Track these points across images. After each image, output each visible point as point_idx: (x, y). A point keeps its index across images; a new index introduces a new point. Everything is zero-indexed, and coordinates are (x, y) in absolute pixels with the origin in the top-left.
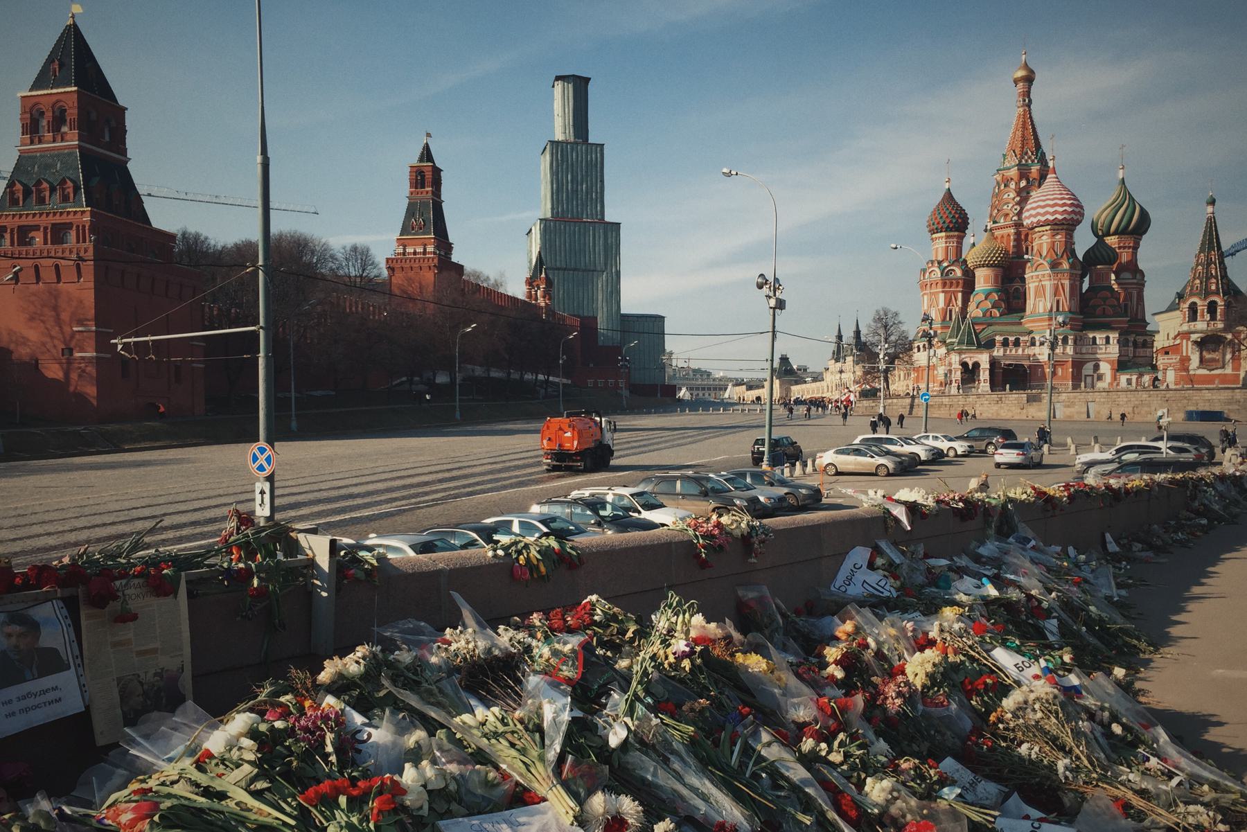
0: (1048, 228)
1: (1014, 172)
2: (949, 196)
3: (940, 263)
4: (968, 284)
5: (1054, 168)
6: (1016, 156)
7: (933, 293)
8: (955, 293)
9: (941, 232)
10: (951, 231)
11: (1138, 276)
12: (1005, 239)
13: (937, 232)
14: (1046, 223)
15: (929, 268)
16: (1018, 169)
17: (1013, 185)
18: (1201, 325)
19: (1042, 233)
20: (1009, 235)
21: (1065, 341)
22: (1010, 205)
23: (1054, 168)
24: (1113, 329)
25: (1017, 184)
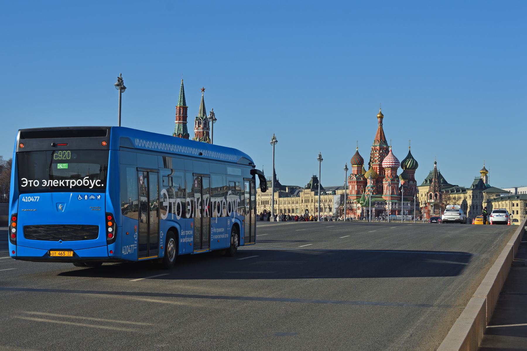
0: (390, 169)
1: (378, 147)
2: (357, 153)
3: (356, 175)
4: (365, 183)
5: (391, 150)
6: (379, 142)
7: (353, 185)
8: (361, 185)
9: (356, 165)
10: (359, 165)
11: (415, 183)
12: (375, 168)
13: (354, 165)
14: (390, 167)
15: (352, 176)
16: (379, 147)
17: (378, 152)
18: (433, 201)
19: (388, 170)
20: (377, 168)
21: (396, 203)
22: (377, 158)
23: (391, 150)
24: (409, 201)
25: (379, 151)
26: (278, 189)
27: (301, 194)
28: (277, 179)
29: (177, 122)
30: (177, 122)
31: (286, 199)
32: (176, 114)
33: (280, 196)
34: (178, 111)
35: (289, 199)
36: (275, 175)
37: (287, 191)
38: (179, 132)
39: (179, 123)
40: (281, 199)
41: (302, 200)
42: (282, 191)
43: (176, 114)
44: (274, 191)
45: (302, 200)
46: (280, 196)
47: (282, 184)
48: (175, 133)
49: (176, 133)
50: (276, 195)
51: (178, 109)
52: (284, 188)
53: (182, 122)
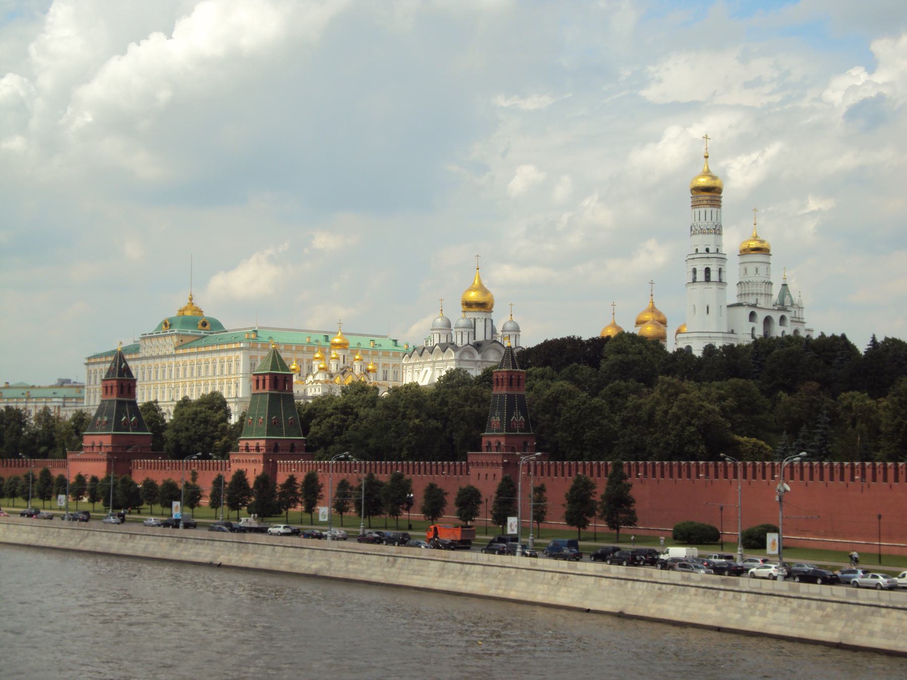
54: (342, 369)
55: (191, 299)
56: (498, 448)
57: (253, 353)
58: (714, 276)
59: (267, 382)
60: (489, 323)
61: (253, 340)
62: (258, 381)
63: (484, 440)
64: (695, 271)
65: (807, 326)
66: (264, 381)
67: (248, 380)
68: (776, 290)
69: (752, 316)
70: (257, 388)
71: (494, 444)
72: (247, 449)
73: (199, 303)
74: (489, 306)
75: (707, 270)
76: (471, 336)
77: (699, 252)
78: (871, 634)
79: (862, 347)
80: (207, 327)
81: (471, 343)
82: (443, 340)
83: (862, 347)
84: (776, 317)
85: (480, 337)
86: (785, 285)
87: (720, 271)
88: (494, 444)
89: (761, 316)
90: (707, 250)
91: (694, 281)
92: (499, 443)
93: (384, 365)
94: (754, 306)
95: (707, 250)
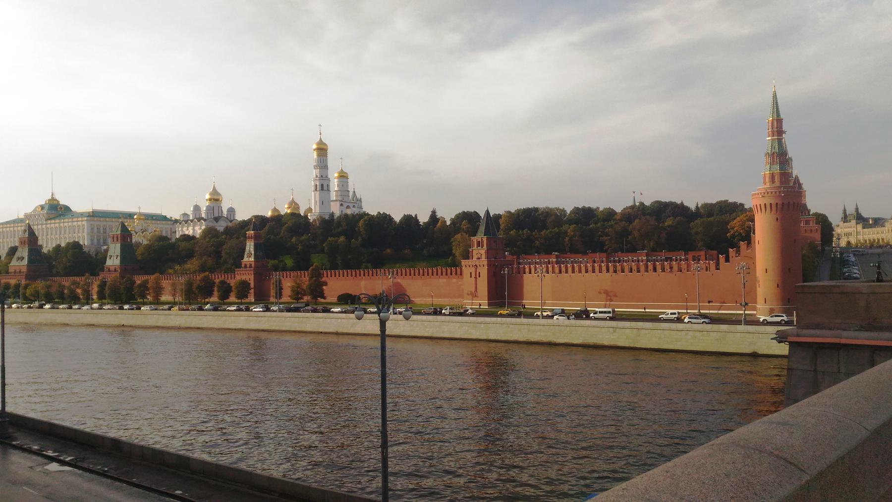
26: (862, 221)
27: (886, 224)
28: (860, 212)
29: (770, 138)
30: (770, 138)
31: (870, 230)
32: (768, 129)
33: (864, 228)
34: (770, 124)
35: (873, 229)
36: (857, 209)
37: (871, 223)
38: (773, 151)
39: (772, 139)
40: (866, 230)
41: (889, 230)
42: (866, 223)
43: (768, 129)
44: (857, 223)
45: (889, 230)
46: (864, 228)
47: (865, 216)
48: (768, 153)
49: (770, 152)
50: (860, 227)
51: (770, 122)
52: (866, 220)
53: (776, 137)
54: (141, 230)
55: (52, 195)
56: (251, 266)
57: (92, 223)
58: (325, 188)
59: (119, 238)
60: (220, 208)
61: (95, 215)
62: (113, 237)
63: (243, 263)
64: (316, 186)
65: (364, 210)
66: (117, 237)
67: (89, 236)
68: (351, 194)
69: (341, 205)
70: (113, 241)
71: (248, 266)
72: (109, 271)
73: (57, 197)
74: (221, 200)
75: (322, 186)
76: (212, 215)
77: (318, 176)
78: (443, 332)
79: (397, 218)
80: (63, 209)
81: (212, 217)
82: (197, 217)
83: (397, 218)
84: (351, 205)
85: (216, 215)
86: (354, 192)
87: (328, 186)
88: (248, 266)
89: (345, 205)
90: (322, 176)
91: (316, 190)
92: (251, 265)
93: (165, 228)
94: (341, 201)
95: (322, 176)
